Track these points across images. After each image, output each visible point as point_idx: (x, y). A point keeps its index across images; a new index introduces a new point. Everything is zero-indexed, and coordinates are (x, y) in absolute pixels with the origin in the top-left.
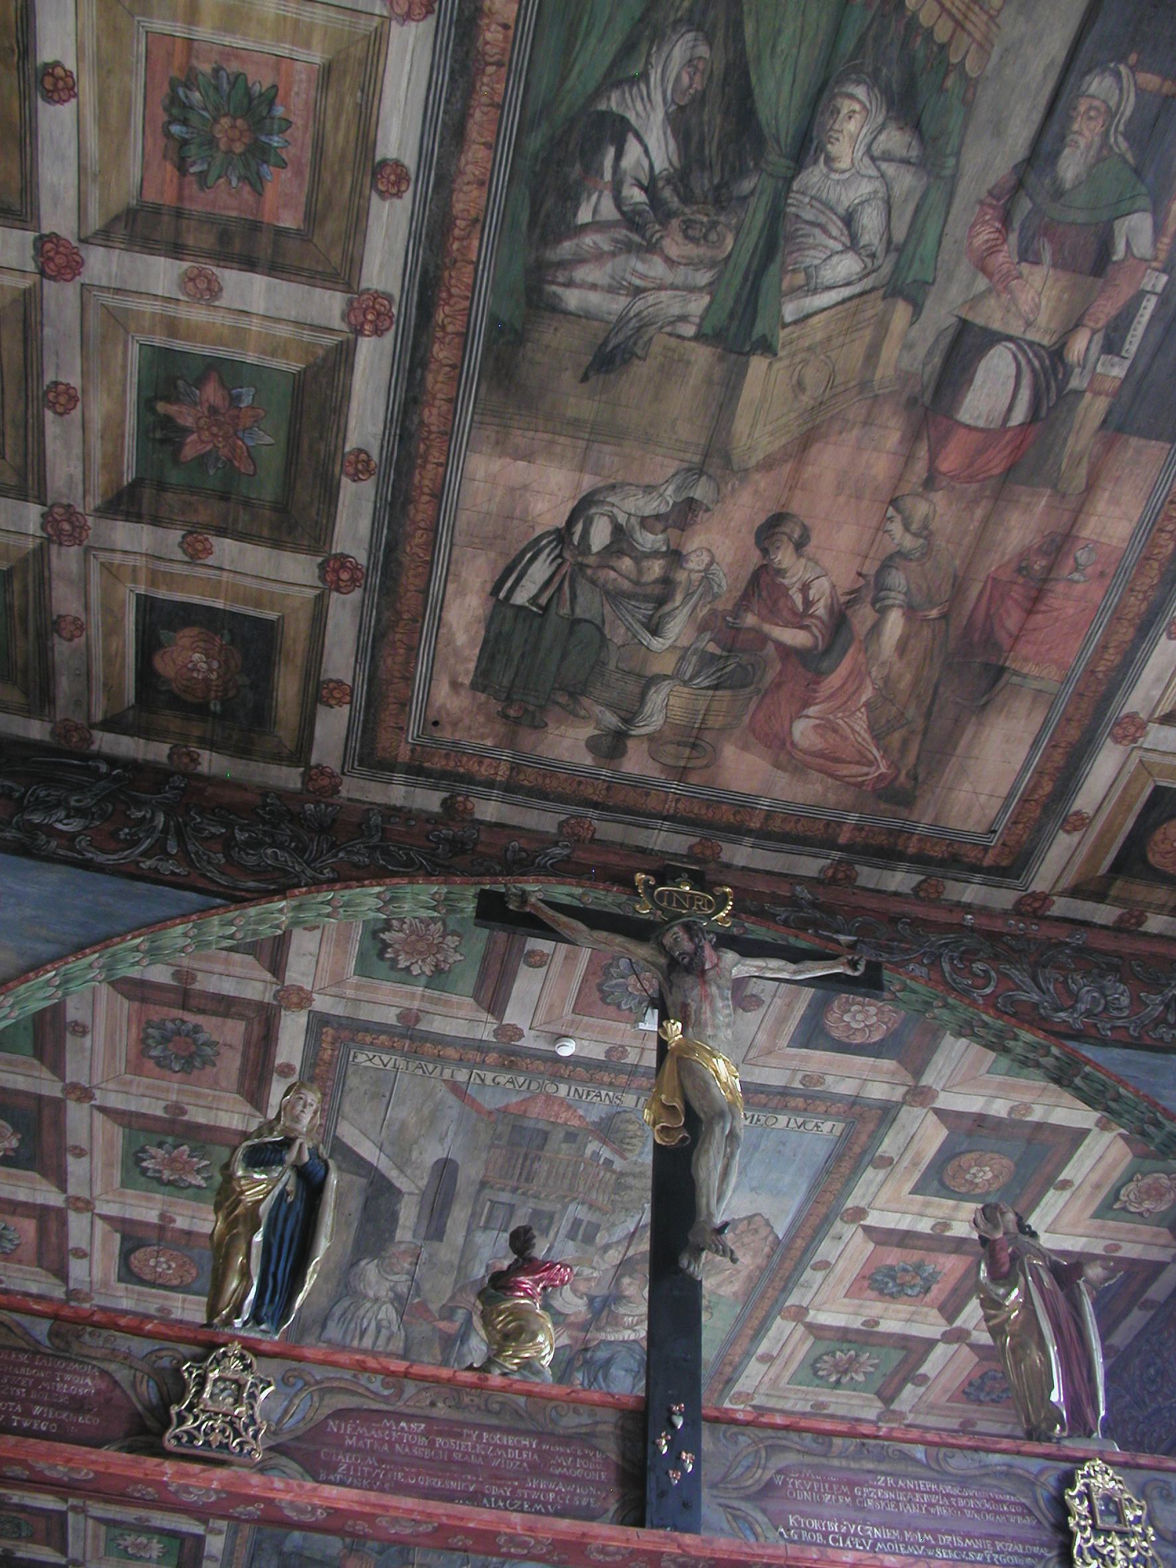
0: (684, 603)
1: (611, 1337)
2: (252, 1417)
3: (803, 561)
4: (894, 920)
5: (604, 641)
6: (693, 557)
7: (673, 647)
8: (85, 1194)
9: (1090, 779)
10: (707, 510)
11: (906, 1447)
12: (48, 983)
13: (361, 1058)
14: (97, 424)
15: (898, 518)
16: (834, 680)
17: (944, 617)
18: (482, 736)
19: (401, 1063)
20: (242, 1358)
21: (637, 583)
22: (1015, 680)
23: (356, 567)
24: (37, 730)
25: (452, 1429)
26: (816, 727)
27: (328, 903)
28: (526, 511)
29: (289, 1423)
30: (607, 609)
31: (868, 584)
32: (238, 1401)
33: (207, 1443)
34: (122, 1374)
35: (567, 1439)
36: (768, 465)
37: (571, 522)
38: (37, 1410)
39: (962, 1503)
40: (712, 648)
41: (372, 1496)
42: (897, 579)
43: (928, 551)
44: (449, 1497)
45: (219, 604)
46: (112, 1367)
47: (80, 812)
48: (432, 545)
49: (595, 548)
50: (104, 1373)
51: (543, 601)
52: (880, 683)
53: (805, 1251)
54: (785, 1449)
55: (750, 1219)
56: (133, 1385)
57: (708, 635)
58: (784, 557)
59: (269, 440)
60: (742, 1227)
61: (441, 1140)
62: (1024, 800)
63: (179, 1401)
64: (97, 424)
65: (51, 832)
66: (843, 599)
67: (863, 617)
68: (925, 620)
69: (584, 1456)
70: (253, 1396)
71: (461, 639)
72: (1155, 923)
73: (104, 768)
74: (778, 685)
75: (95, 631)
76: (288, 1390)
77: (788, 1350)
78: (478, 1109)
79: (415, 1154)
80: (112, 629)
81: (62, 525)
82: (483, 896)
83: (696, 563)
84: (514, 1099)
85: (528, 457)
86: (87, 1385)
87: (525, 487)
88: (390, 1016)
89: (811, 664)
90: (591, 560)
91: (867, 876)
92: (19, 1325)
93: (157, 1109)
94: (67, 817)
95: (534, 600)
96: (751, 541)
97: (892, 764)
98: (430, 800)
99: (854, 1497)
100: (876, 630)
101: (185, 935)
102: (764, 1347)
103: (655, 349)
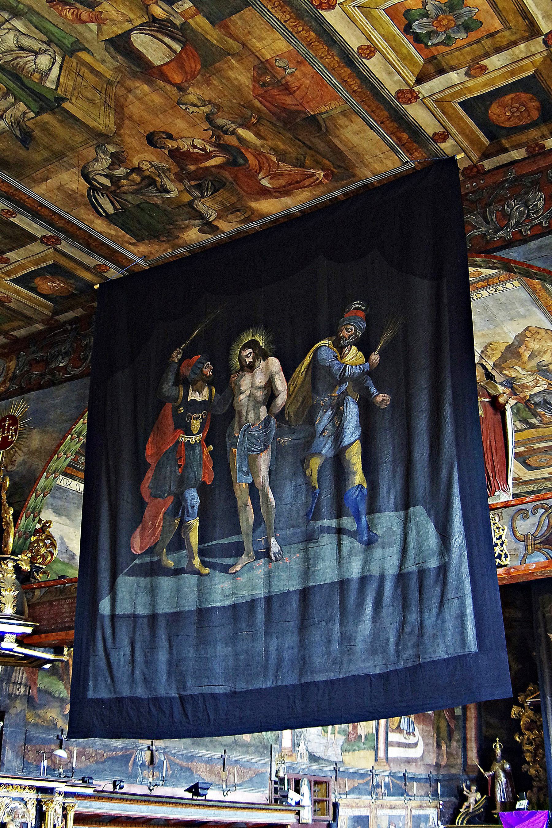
0: (162, 179)
12: (71, 439)
15: (189, 107)
18: (165, 250)
21: (137, 184)
23: (51, 237)
24: (39, 327)
28: (72, 190)
30: (141, 197)
36: (119, 126)
37: (89, 182)
42: (221, 121)
43: (218, 107)
47: (67, 354)
49: (110, 185)
55: (527, 329)
58: (171, 144)
65: (58, 368)
68: (253, 125)
73: (69, 327)
74: (236, 179)
80: (17, 293)
83: (145, 166)
85: (48, 178)
87: (61, 185)
90: (113, 188)
94: (63, 359)
95: (115, 208)
100: (240, 139)
103: (32, 126)
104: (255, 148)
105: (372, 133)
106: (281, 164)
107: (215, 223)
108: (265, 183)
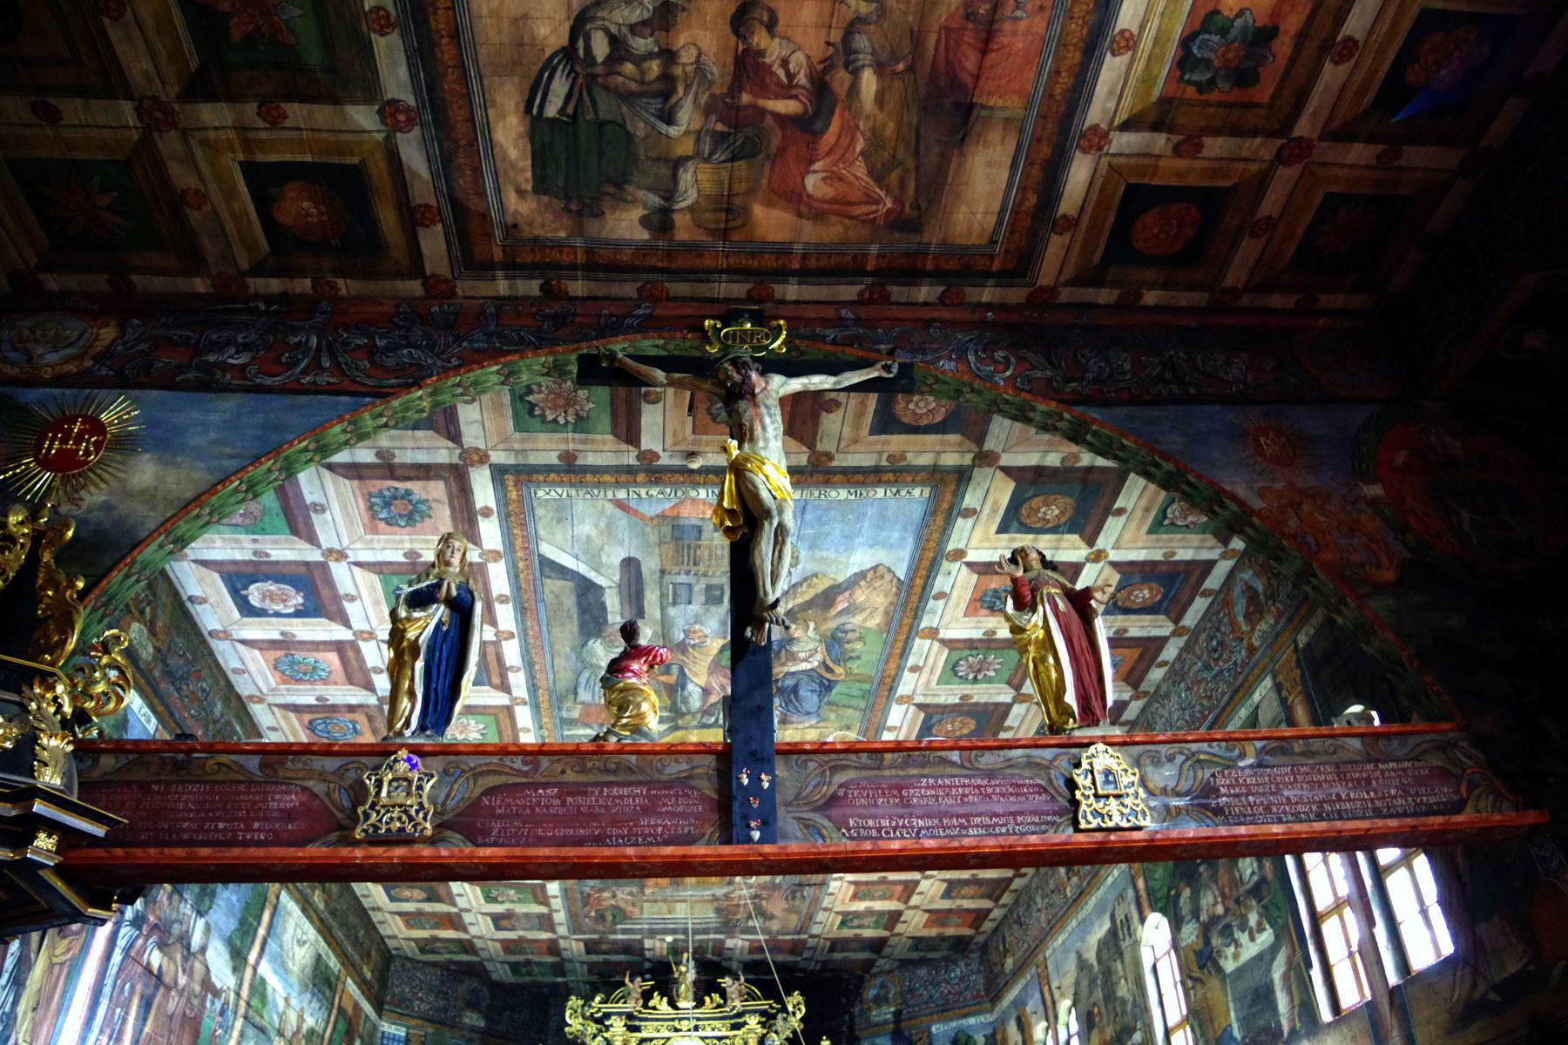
0: (686, 93)
1: (793, 669)
2: (421, 804)
3: (777, 40)
4: (927, 323)
5: (629, 138)
6: (683, 53)
7: (687, 132)
8: (366, 627)
9: (1069, 187)
10: (684, 9)
11: (943, 754)
12: (236, 490)
13: (541, 493)
14: (150, 24)
16: (830, 137)
17: (910, 69)
18: (556, 231)
19: (573, 492)
20: (409, 760)
21: (642, 82)
22: (984, 113)
23: (408, 109)
24: (200, 285)
25: (579, 790)
26: (824, 179)
27: (459, 385)
28: (533, 37)
29: (451, 804)
30: (624, 109)
31: (837, 50)
32: (409, 794)
33: (388, 830)
34: (318, 788)
35: (669, 785)
38: (256, 825)
39: (990, 790)
40: (720, 127)
41: (517, 851)
42: (862, 42)
44: (579, 842)
45: (308, 158)
46: (310, 784)
47: (246, 347)
48: (464, 78)
49: (600, 59)
50: (304, 789)
51: (570, 110)
52: (869, 134)
53: (924, 588)
54: (846, 767)
55: (875, 568)
56: (328, 794)
57: (714, 118)
58: (760, 39)
59: (298, 12)
60: (870, 576)
61: (621, 543)
62: (1015, 212)
63: (363, 804)
64: (150, 24)
65: (225, 367)
66: (820, 67)
67: (840, 80)
68: (894, 74)
69: (686, 795)
70: (420, 788)
71: (513, 154)
72: (1151, 298)
73: (262, 307)
74: (783, 150)
75: (216, 198)
76: (448, 779)
77: (931, 661)
78: (643, 517)
79: (604, 559)
80: (230, 194)
81: (155, 115)
82: (583, 360)
83: (687, 57)
84: (668, 505)
86: (293, 800)
87: (525, 16)
88: (553, 458)
89: (807, 126)
90: (599, 70)
91: (897, 292)
92: (235, 763)
93: (398, 557)
94: (237, 352)
95: (562, 111)
96: (728, 29)
97: (896, 200)
98: (532, 287)
99: (902, 797)
100: (854, 89)
101: (344, 431)
102: (911, 662)
104: (856, 115)
105: (1005, 174)
106: (860, 163)
107: (677, 217)
108: (811, 182)
